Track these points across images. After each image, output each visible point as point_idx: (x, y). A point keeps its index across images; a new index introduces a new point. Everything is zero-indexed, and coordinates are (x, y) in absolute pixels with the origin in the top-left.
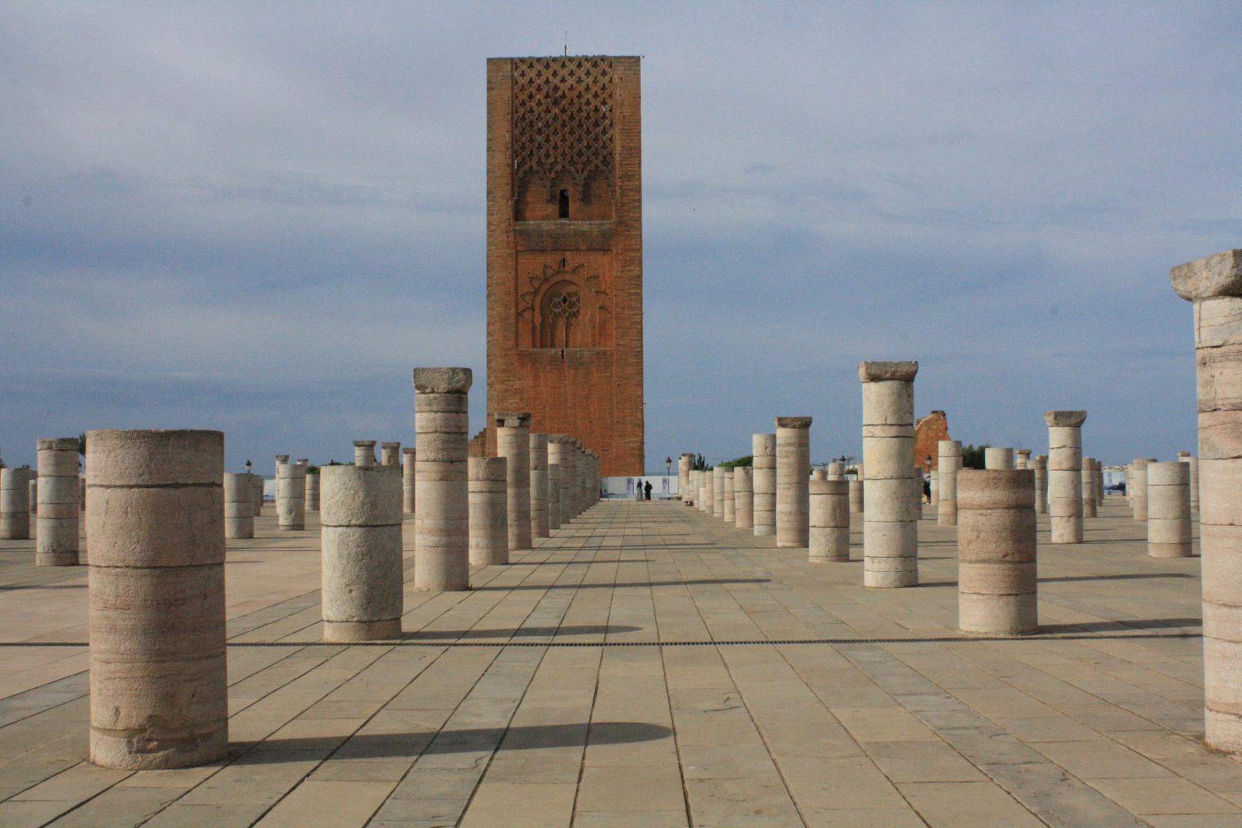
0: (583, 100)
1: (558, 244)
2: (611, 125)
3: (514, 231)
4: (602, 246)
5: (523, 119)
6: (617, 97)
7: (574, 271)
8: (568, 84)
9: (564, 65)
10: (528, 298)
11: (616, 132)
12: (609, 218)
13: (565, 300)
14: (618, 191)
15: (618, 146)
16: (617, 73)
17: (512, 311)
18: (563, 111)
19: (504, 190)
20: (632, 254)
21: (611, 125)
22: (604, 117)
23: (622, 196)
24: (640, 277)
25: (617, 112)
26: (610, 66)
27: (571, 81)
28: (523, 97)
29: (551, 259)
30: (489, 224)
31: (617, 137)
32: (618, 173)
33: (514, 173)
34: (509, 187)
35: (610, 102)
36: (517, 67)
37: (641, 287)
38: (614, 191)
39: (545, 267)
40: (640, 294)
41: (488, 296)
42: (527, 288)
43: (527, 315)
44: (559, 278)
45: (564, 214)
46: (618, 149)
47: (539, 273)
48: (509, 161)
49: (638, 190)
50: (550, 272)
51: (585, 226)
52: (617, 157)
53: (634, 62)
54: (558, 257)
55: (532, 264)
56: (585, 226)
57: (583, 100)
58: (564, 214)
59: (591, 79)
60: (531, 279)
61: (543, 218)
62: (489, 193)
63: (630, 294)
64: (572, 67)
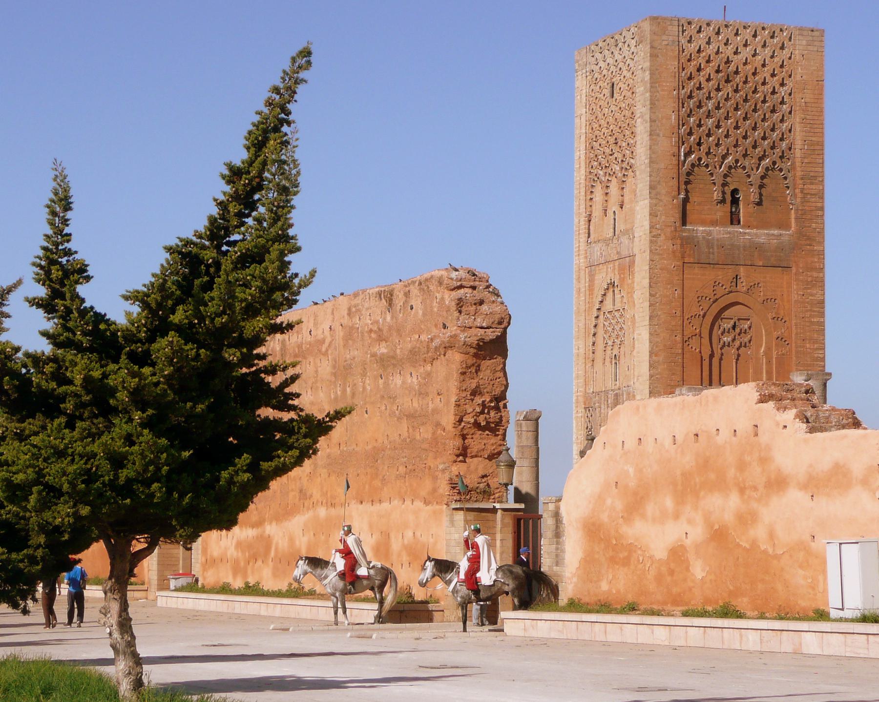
0: (759, 78)
1: (729, 258)
2: (790, 113)
3: (682, 238)
4: (779, 262)
5: (690, 97)
6: (798, 78)
7: (747, 292)
8: (741, 57)
9: (737, 34)
10: (696, 322)
11: (796, 120)
12: (787, 227)
13: (734, 327)
14: (799, 195)
15: (798, 137)
16: (798, 47)
17: (679, 338)
18: (736, 91)
19: (668, 187)
20: (815, 274)
21: (790, 113)
22: (782, 102)
23: (804, 201)
24: (822, 302)
25: (797, 96)
26: (790, 39)
27: (746, 53)
28: (691, 68)
29: (723, 275)
30: (652, 227)
31: (798, 128)
32: (799, 174)
33: (680, 164)
34: (675, 181)
35: (790, 84)
36: (683, 31)
37: (822, 315)
38: (794, 195)
39: (716, 284)
40: (822, 324)
41: (651, 318)
42: (696, 310)
43: (694, 343)
44: (732, 298)
45: (734, 219)
46: (798, 144)
47: (709, 292)
48: (675, 150)
49: (821, 196)
50: (720, 291)
51: (762, 236)
52: (798, 153)
53: (816, 35)
54: (731, 275)
55: (701, 280)
56: (762, 236)
57: (759, 78)
58: (734, 219)
59: (768, 51)
60: (700, 299)
61: (714, 223)
62: (652, 188)
63: (812, 323)
64: (747, 34)
